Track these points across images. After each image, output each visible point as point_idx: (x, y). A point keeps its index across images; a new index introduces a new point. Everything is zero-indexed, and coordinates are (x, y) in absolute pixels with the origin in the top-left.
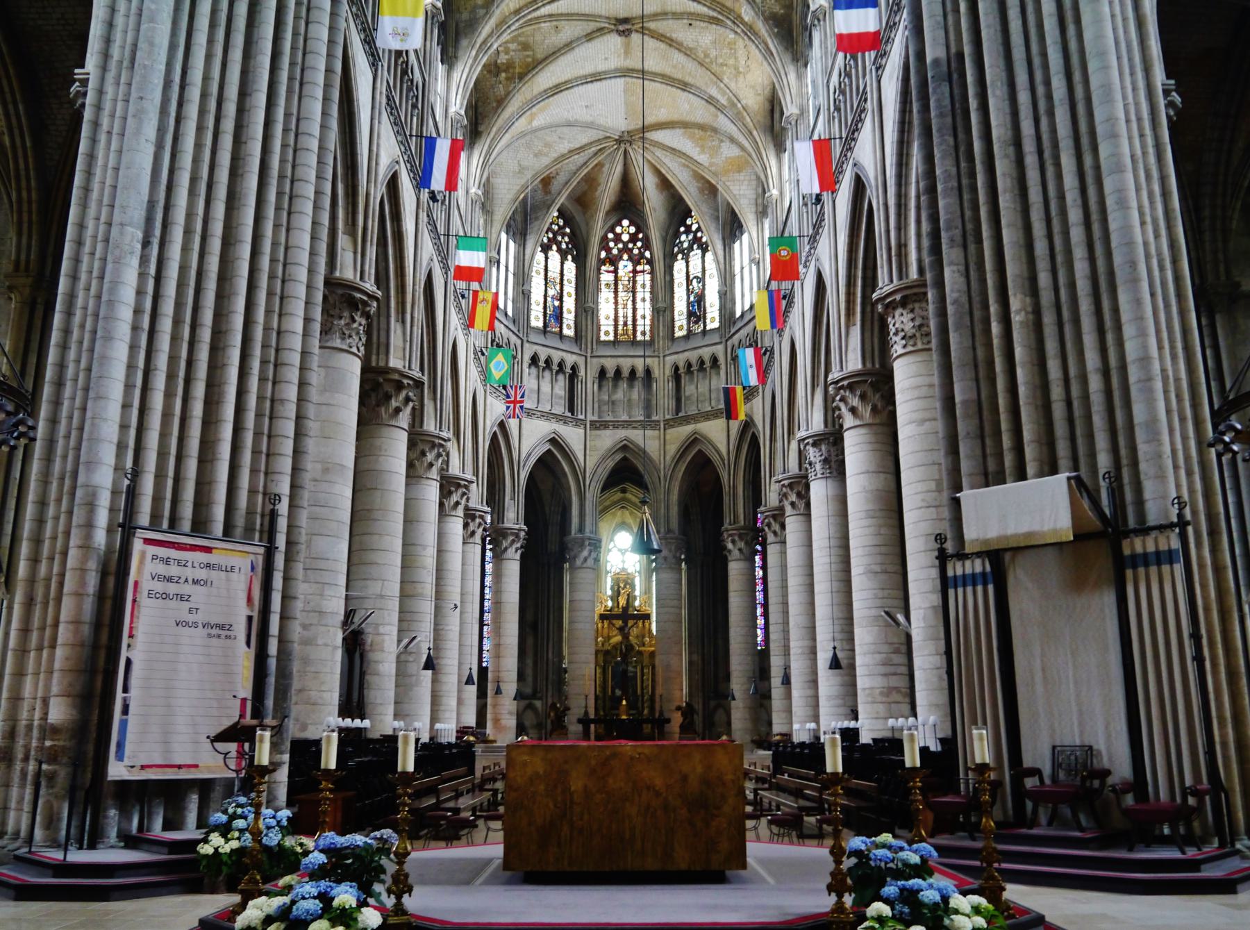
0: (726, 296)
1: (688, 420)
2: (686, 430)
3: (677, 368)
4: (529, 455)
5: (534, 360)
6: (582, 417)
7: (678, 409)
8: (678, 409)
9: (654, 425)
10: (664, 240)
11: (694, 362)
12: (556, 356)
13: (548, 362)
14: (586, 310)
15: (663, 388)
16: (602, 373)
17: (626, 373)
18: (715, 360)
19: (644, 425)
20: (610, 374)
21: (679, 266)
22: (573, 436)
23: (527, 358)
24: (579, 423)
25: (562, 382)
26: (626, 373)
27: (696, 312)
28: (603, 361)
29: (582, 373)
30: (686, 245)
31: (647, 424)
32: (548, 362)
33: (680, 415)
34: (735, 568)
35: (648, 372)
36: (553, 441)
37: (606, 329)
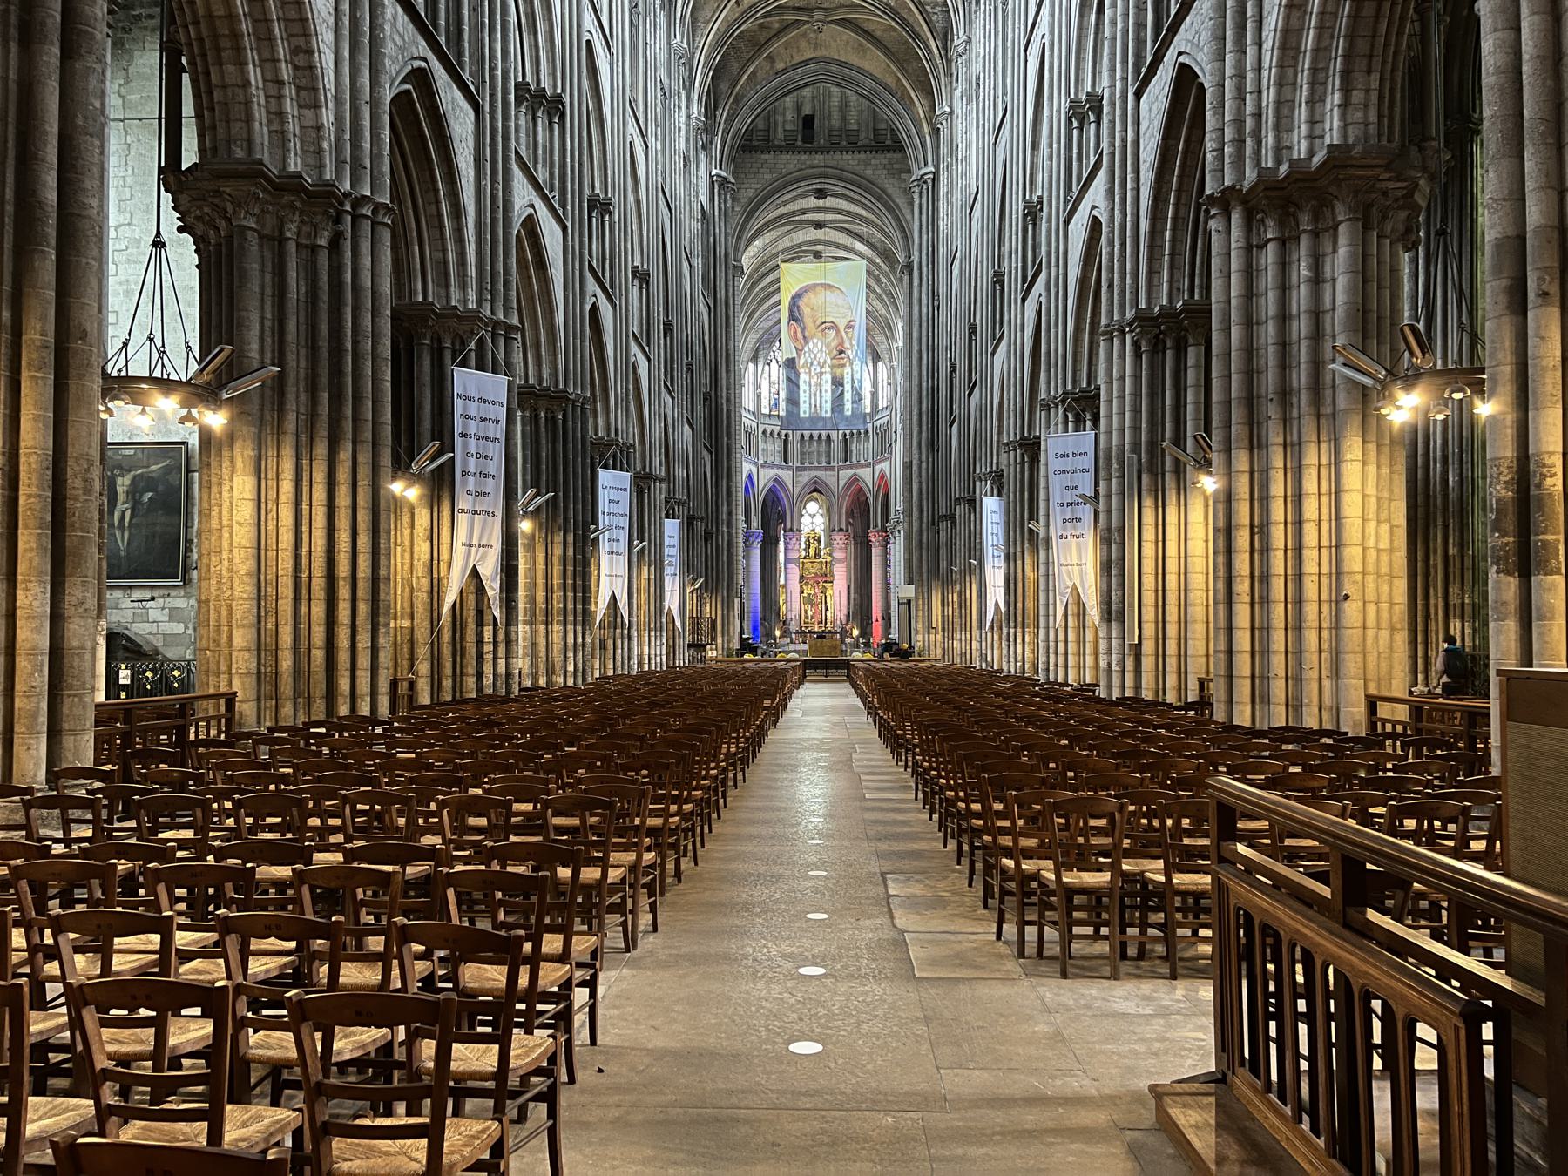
0: (874, 395)
1: (851, 467)
2: (851, 472)
5: (764, 432)
13: (772, 433)
14: (793, 401)
15: (837, 447)
16: (802, 436)
19: (826, 469)
20: (807, 438)
22: (786, 476)
24: (789, 468)
25: (778, 443)
27: (858, 398)
31: (829, 468)
32: (772, 433)
35: (829, 436)
36: (775, 480)
37: (804, 410)
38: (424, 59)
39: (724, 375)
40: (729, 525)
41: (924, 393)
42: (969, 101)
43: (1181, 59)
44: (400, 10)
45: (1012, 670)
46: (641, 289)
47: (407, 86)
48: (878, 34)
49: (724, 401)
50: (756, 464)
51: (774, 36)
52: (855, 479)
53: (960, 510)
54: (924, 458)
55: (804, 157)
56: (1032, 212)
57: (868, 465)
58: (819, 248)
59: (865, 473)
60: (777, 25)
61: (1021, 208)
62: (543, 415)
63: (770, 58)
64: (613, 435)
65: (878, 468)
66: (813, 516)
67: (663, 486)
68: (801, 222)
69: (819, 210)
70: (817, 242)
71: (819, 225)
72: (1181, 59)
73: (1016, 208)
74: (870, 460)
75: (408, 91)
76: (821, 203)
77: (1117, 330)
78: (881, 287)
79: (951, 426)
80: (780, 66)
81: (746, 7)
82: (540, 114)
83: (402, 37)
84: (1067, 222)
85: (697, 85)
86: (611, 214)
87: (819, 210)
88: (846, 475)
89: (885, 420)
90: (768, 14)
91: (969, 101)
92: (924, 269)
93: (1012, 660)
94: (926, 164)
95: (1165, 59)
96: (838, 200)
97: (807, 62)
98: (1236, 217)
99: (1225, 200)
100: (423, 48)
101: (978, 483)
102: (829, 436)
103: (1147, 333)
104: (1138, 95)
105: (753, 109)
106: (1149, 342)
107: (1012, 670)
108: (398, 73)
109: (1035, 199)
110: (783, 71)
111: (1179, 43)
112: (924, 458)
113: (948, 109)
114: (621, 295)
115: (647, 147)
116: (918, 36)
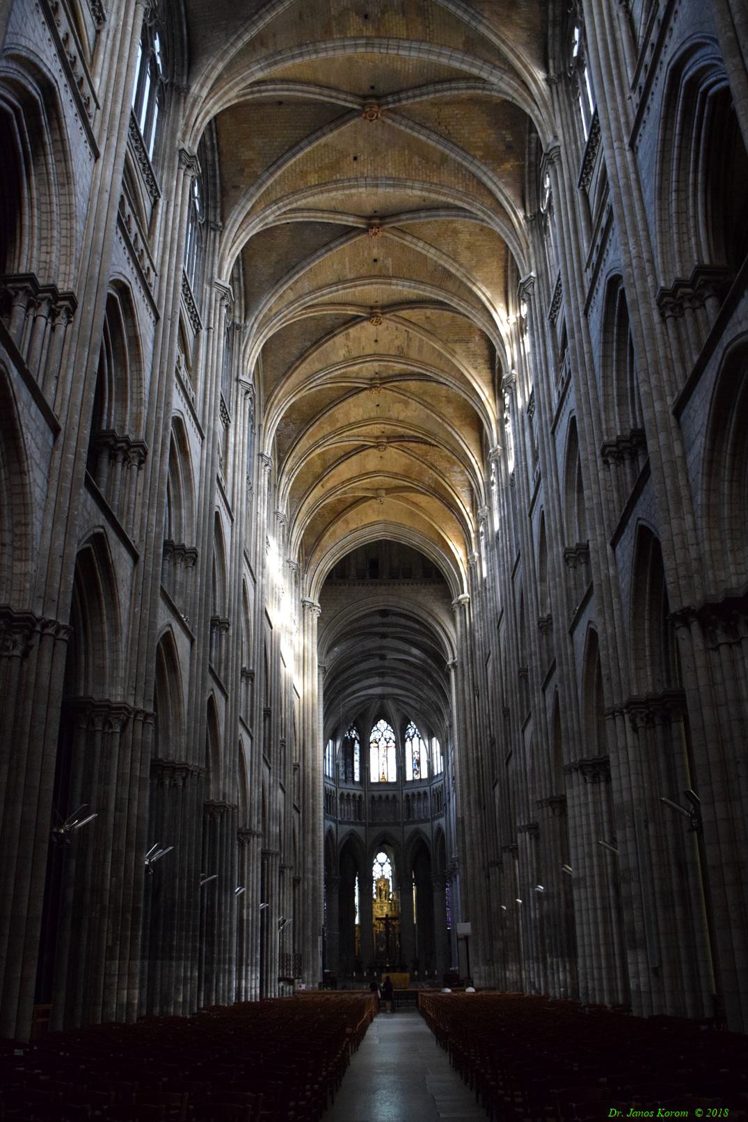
1: (414, 822)
2: (414, 827)
3: (407, 796)
4: (342, 841)
5: (342, 795)
6: (364, 821)
7: (409, 816)
8: (409, 816)
9: (398, 824)
10: (401, 731)
11: (416, 794)
12: (352, 792)
17: (384, 797)
18: (425, 793)
21: (408, 744)
22: (360, 830)
23: (338, 795)
24: (362, 824)
26: (384, 797)
28: (374, 793)
29: (364, 799)
30: (411, 735)
33: (411, 819)
34: (436, 895)
37: (374, 778)
38: (103, 527)
39: (310, 749)
40: (314, 873)
41: (471, 762)
42: (492, 549)
43: (640, 522)
44: (89, 496)
45: (558, 995)
46: (247, 684)
47: (88, 545)
48: (423, 504)
49: (310, 770)
50: (335, 821)
51: (349, 507)
52: (417, 832)
53: (506, 857)
54: (473, 814)
55: (371, 588)
56: (545, 626)
57: (427, 821)
58: (383, 652)
59: (426, 828)
60: (351, 500)
61: (536, 623)
62: (167, 782)
63: (347, 522)
64: (221, 799)
65: (436, 822)
66: (382, 865)
67: (260, 840)
68: (371, 633)
69: (383, 625)
70: (382, 648)
71: (384, 636)
72: (640, 522)
73: (533, 623)
74: (429, 817)
75: (89, 549)
76: (385, 620)
77: (618, 712)
78: (432, 681)
79: (494, 788)
80: (353, 526)
81: (329, 488)
82: (179, 561)
83: (89, 513)
84: (571, 633)
85: (293, 540)
86: (227, 630)
87: (383, 625)
88: (410, 829)
89: (440, 783)
90: (345, 493)
91: (492, 549)
92: (466, 667)
93: (556, 986)
94: (463, 593)
95: (630, 521)
96: (398, 618)
97: (372, 524)
98: (695, 626)
99: (685, 616)
100: (102, 520)
101: (519, 835)
102: (394, 796)
103: (641, 713)
104: (613, 545)
105: (334, 555)
106: (642, 719)
107: (558, 995)
108: (83, 537)
109: (545, 616)
110: (356, 530)
111: (639, 511)
112: (473, 814)
113: (476, 554)
114: (232, 689)
115: (255, 582)
116: (452, 506)
